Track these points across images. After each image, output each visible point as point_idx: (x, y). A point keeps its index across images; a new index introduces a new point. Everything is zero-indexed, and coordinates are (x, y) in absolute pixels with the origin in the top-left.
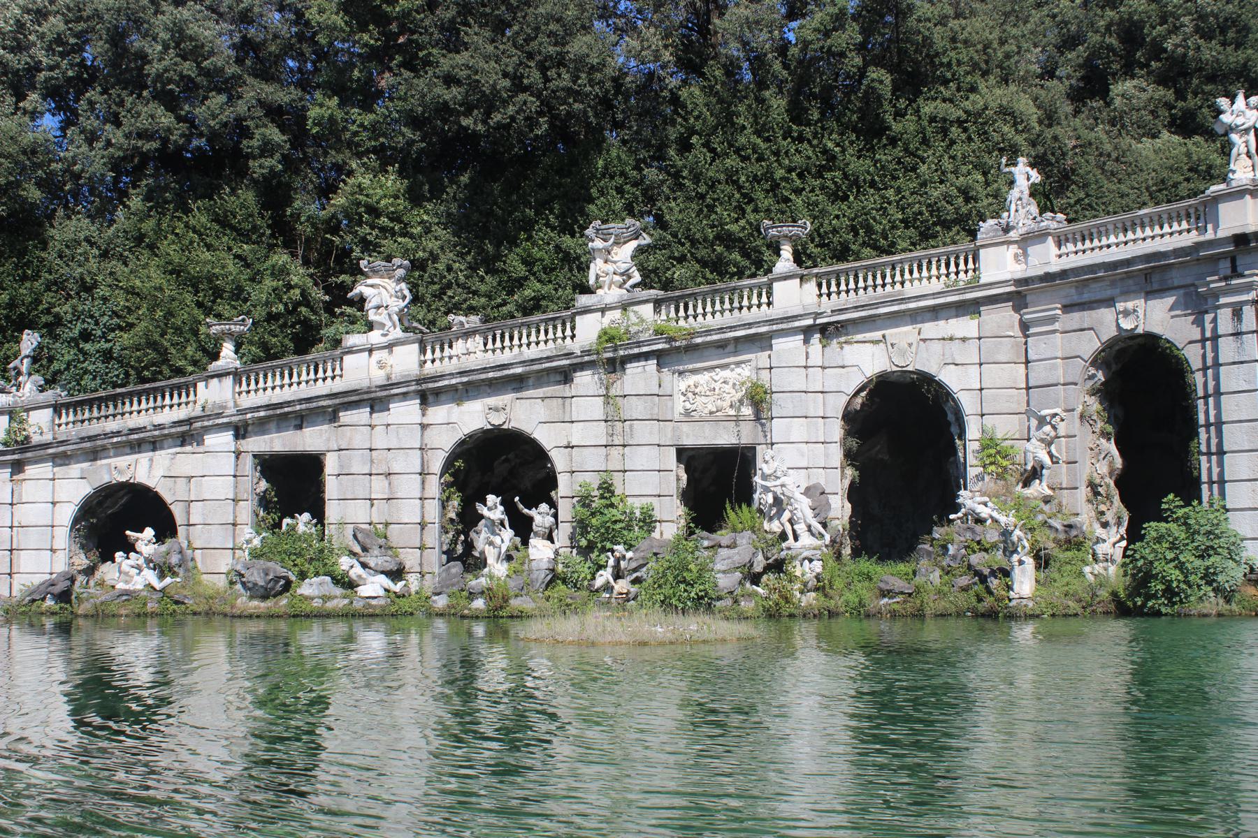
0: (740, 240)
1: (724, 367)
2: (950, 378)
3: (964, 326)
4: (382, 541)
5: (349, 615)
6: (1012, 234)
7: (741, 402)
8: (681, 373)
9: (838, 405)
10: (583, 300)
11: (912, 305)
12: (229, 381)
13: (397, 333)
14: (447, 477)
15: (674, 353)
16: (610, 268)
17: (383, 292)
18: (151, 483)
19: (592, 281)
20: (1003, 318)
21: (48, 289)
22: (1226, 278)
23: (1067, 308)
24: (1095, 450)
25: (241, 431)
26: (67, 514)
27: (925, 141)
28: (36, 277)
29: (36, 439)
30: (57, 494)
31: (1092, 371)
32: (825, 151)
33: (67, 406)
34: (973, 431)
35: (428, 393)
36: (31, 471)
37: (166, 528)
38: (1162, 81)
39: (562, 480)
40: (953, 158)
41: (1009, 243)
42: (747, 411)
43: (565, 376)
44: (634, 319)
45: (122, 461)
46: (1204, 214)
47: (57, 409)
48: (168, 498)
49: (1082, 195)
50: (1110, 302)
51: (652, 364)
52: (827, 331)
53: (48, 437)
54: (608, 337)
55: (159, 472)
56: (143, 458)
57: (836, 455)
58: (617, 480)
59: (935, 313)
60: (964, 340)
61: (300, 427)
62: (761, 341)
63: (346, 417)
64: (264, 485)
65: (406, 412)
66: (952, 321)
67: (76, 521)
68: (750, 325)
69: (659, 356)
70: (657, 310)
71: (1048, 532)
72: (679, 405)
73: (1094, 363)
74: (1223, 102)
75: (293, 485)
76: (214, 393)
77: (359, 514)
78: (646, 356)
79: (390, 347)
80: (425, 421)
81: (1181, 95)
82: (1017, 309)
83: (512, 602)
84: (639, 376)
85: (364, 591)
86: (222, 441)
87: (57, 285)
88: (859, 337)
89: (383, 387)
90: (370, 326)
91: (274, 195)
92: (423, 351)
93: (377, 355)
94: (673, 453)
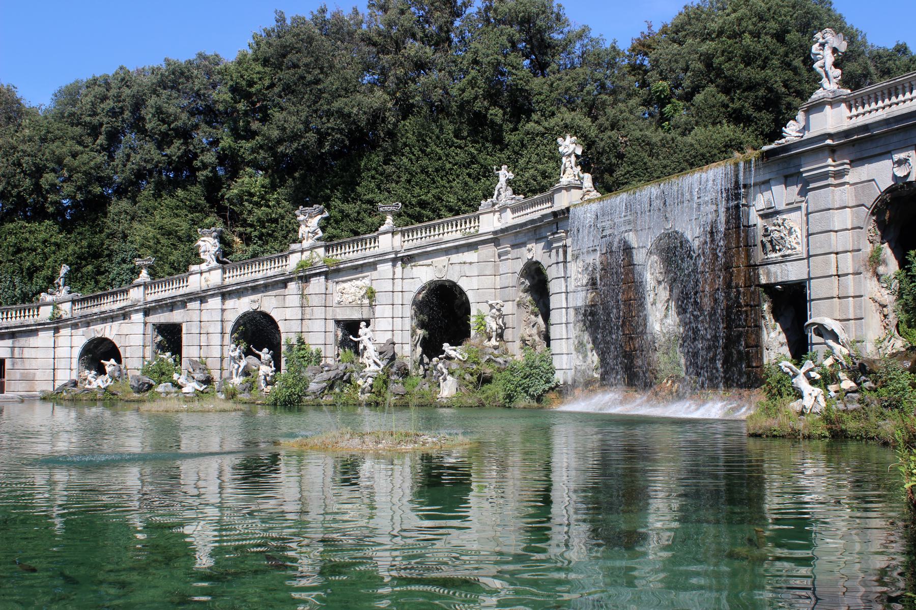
0: (429, 204)
1: (357, 279)
2: (463, 284)
3: (470, 256)
4: (202, 366)
6: (496, 207)
7: (363, 297)
8: (337, 283)
9: (409, 298)
10: (294, 246)
11: (443, 246)
12: (142, 288)
13: (214, 263)
14: (236, 335)
15: (333, 273)
16: (307, 229)
17: (208, 245)
18: (111, 338)
19: (300, 236)
20: (489, 251)
21: (108, 237)
22: (553, 234)
23: (514, 246)
24: (527, 322)
25: (147, 312)
26: (77, 352)
27: (523, 146)
28: (101, 232)
29: (64, 317)
30: (73, 342)
31: (523, 280)
32: (471, 154)
33: (78, 301)
34: (474, 312)
35: (225, 294)
36: (63, 332)
38: (726, 91)
40: (538, 154)
41: (494, 212)
42: (366, 301)
43: (284, 284)
44: (315, 255)
45: (99, 327)
46: (551, 199)
47: (74, 302)
49: (631, 168)
50: (524, 244)
51: (322, 278)
52: (407, 260)
53: (69, 316)
54: (302, 266)
55: (114, 332)
56: (108, 325)
57: (408, 324)
58: (304, 336)
59: (457, 249)
60: (471, 263)
61: (172, 311)
62: (373, 266)
63: (190, 305)
64: (160, 338)
65: (215, 303)
66: (466, 254)
67: (81, 355)
68: (365, 258)
69: (327, 275)
70: (327, 250)
71: (493, 364)
72: (337, 298)
73: (522, 276)
74: (560, 140)
75: (171, 337)
76: (136, 294)
78: (319, 274)
79: (209, 270)
80: (224, 307)
81: (732, 100)
82: (496, 246)
83: (239, 396)
84: (317, 284)
85: (184, 390)
86: (138, 317)
87: (112, 235)
88: (421, 263)
89: (204, 291)
90: (202, 261)
91: (213, 187)
92: (224, 272)
93: (204, 275)
94: (332, 322)
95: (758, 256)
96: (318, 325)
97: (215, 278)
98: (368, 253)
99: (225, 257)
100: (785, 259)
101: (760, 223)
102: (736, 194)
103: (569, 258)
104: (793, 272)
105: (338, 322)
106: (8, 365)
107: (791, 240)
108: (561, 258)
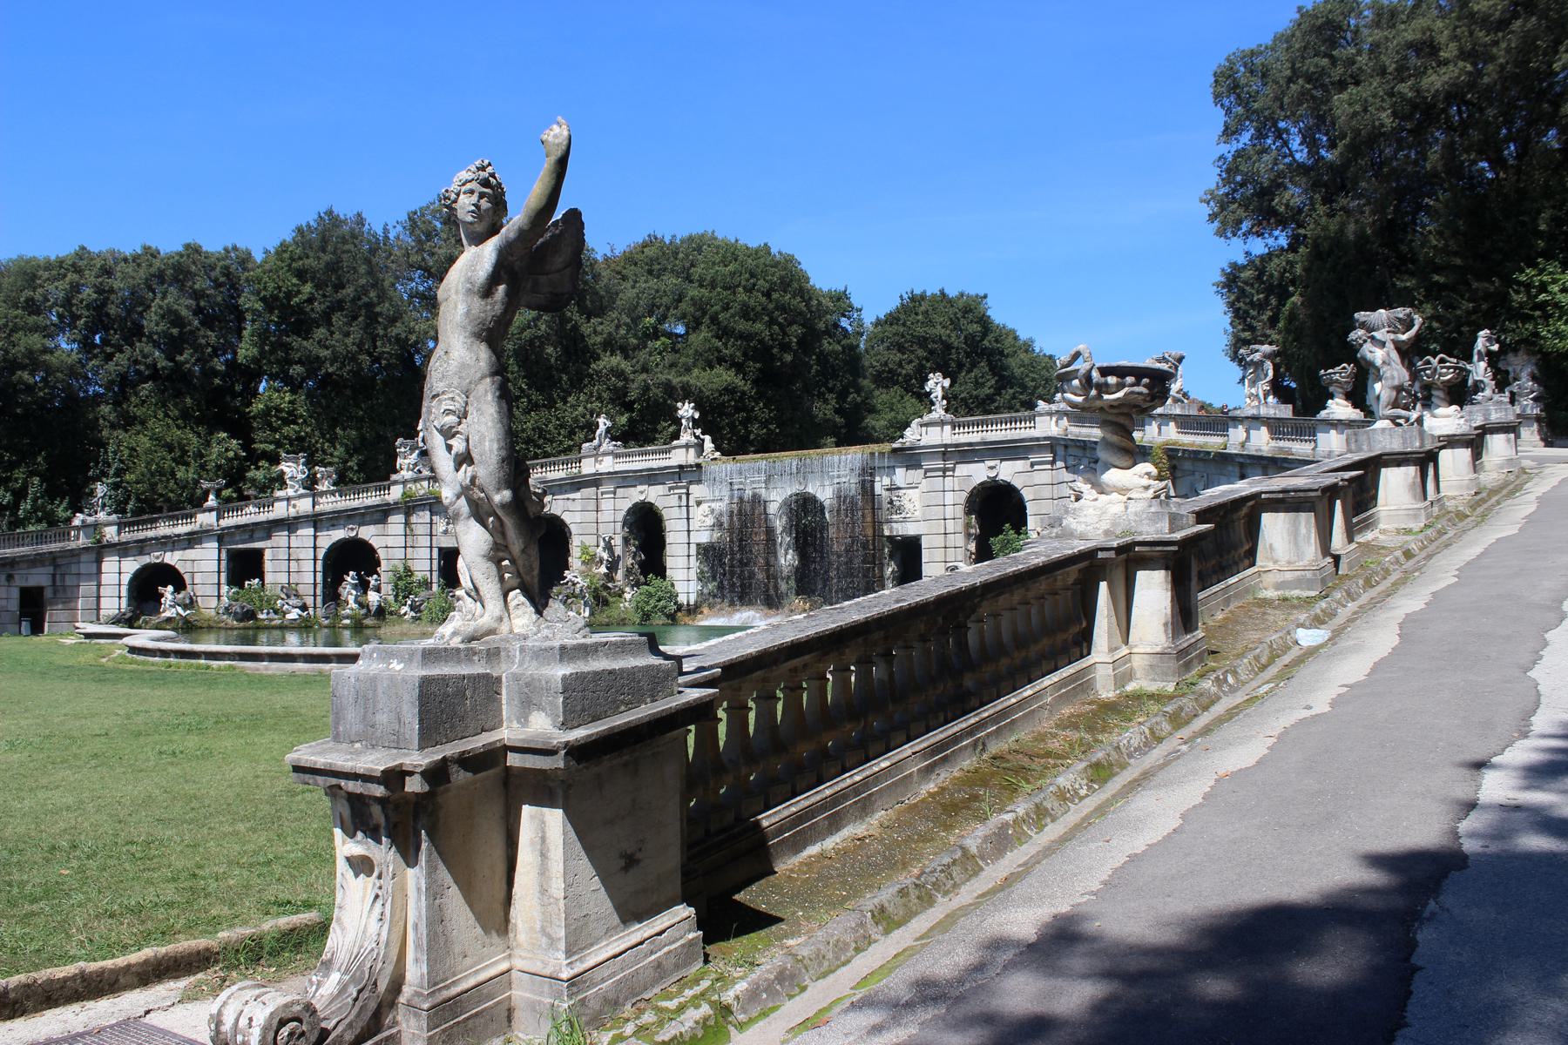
2: (567, 518)
5: (282, 628)
25: (222, 537)
35: (317, 521)
37: (180, 585)
39: (383, 563)
48: (182, 571)
58: (410, 563)
75: (244, 566)
76: (205, 519)
77: (283, 579)
85: (289, 616)
95: (883, 514)
96: (425, 553)
97: (305, 506)
99: (310, 483)
101: (885, 494)
102: (867, 474)
103: (691, 503)
104: (910, 530)
105: (440, 549)
106: (48, 594)
107: (908, 506)
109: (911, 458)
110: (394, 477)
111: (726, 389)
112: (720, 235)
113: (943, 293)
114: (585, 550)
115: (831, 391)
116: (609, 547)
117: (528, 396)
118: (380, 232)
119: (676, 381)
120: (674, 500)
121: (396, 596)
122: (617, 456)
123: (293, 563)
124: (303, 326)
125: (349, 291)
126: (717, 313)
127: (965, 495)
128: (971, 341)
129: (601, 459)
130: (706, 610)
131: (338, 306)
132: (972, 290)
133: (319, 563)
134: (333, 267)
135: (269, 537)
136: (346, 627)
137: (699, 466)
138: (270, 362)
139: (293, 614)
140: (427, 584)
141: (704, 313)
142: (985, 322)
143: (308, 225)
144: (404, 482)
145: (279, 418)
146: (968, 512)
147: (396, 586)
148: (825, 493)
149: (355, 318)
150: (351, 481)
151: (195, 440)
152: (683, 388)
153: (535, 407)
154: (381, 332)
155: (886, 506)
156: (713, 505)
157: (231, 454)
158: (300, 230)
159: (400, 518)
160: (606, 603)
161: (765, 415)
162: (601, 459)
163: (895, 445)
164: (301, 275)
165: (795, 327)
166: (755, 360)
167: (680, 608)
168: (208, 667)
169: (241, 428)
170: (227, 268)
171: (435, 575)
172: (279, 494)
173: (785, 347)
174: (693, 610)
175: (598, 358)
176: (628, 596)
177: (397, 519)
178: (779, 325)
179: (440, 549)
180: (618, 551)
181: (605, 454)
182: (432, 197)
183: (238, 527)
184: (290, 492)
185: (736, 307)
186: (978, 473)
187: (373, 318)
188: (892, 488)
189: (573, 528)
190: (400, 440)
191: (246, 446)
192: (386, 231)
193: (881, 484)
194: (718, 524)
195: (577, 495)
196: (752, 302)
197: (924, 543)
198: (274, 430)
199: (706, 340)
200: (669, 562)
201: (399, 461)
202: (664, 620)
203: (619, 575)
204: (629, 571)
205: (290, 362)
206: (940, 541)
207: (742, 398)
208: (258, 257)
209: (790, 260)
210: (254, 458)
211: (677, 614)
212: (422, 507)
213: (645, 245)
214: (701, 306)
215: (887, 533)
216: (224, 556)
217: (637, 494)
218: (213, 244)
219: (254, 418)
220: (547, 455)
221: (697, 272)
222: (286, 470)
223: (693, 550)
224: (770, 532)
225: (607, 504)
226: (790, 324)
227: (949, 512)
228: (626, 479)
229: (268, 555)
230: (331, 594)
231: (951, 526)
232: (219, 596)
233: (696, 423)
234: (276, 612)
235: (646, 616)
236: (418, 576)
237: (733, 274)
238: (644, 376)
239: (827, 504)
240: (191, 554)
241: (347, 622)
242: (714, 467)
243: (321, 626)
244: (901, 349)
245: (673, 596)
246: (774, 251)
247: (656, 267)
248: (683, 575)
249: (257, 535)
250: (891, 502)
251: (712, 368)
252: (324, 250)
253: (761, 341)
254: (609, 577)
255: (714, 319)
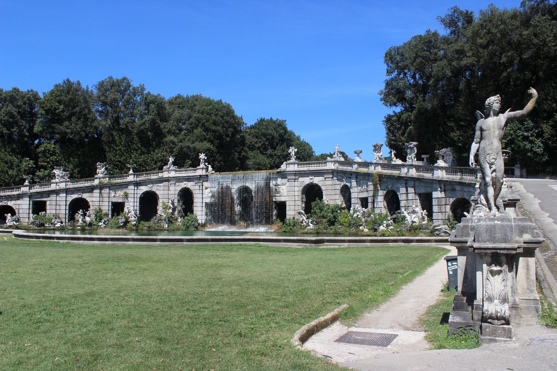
2: (157, 192)
9: (139, 196)
25: (31, 196)
35: (67, 191)
37: (13, 212)
39: (91, 207)
48: (14, 208)
76: (24, 189)
85: (56, 226)
95: (273, 194)
96: (107, 204)
97: (62, 186)
98: (125, 180)
100: (281, 196)
104: (283, 199)
105: (112, 202)
107: (282, 191)
108: (201, 188)
109: (283, 175)
110: (96, 176)
111: (207, 149)
112: (204, 96)
113: (271, 119)
114: (164, 203)
115: (236, 151)
116: (173, 203)
117: (141, 149)
118: (85, 88)
119: (191, 146)
120: (197, 187)
121: (96, 219)
122: (176, 171)
123: (58, 206)
124: (60, 121)
125: (78, 109)
126: (204, 123)
127: (302, 188)
128: (281, 136)
129: (170, 172)
130: (208, 226)
131: (73, 114)
132: (281, 118)
133: (67, 207)
134: (71, 100)
135: (49, 197)
136: (79, 230)
137: (207, 176)
138: (47, 133)
139: (58, 225)
140: (107, 215)
141: (199, 122)
142: (285, 129)
143: (60, 84)
144: (100, 178)
145: (49, 154)
146: (302, 194)
147: (96, 215)
148: (252, 186)
149: (79, 119)
150: (75, 177)
151: (16, 160)
152: (193, 148)
153: (142, 153)
154: (89, 124)
155: (274, 191)
156: (212, 189)
157: (30, 166)
158: (56, 86)
159: (98, 191)
160: (172, 222)
161: (220, 159)
162: (170, 172)
163: (278, 170)
164: (60, 102)
165: (230, 129)
166: (217, 139)
167: (199, 224)
168: (58, 242)
169: (35, 158)
170: (29, 98)
171: (110, 211)
172: (53, 181)
173: (227, 136)
174: (204, 225)
175: (166, 137)
176: (179, 220)
177: (97, 191)
178: (226, 128)
179: (112, 202)
180: (176, 204)
181: (172, 170)
182: (107, 77)
183: (37, 193)
184: (57, 180)
185: (211, 121)
186: (307, 180)
187: (86, 119)
188: (276, 185)
189: (160, 196)
190: (98, 163)
191: (36, 163)
192: (87, 88)
193: (272, 183)
194: (213, 196)
195: (162, 185)
196: (217, 120)
197: (287, 204)
198: (48, 158)
199: (200, 132)
200: (195, 209)
201: (98, 170)
202: (194, 229)
203: (176, 213)
204: (179, 212)
205: (55, 133)
206: (293, 203)
207: (212, 153)
208: (41, 96)
209: (229, 105)
210: (39, 168)
211: (199, 227)
212: (106, 187)
213: (176, 98)
214: (198, 120)
215: (274, 200)
216: (31, 203)
217: (184, 185)
218: (24, 88)
219: (40, 153)
220: (147, 170)
221: (197, 108)
222: (56, 172)
223: (204, 205)
224: (232, 199)
225: (172, 188)
226: (229, 127)
227: (296, 193)
228: (179, 180)
229: (48, 203)
230: (72, 218)
231: (297, 198)
232: (29, 218)
233: (205, 161)
234: (52, 224)
235: (188, 227)
236: (104, 212)
237: (210, 109)
238: (181, 144)
239: (253, 190)
240: (18, 202)
241: (79, 228)
242: (213, 176)
243: (68, 229)
244: (257, 137)
245: (197, 221)
246: (223, 102)
247: (181, 106)
248: (200, 213)
249: (44, 196)
250: (276, 190)
251: (202, 142)
252: (68, 93)
253: (220, 133)
254: (173, 214)
255: (203, 125)
